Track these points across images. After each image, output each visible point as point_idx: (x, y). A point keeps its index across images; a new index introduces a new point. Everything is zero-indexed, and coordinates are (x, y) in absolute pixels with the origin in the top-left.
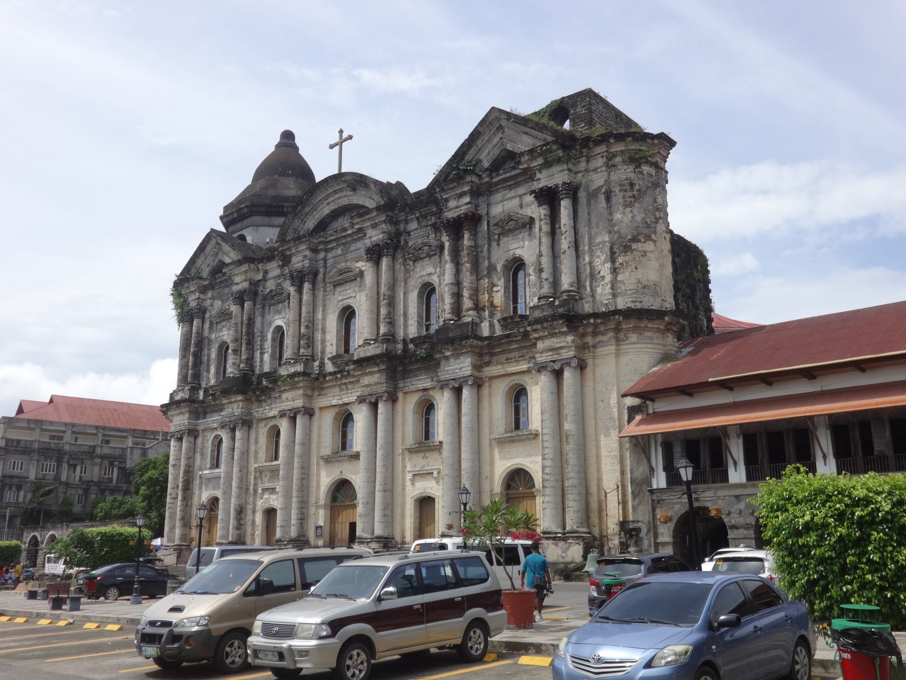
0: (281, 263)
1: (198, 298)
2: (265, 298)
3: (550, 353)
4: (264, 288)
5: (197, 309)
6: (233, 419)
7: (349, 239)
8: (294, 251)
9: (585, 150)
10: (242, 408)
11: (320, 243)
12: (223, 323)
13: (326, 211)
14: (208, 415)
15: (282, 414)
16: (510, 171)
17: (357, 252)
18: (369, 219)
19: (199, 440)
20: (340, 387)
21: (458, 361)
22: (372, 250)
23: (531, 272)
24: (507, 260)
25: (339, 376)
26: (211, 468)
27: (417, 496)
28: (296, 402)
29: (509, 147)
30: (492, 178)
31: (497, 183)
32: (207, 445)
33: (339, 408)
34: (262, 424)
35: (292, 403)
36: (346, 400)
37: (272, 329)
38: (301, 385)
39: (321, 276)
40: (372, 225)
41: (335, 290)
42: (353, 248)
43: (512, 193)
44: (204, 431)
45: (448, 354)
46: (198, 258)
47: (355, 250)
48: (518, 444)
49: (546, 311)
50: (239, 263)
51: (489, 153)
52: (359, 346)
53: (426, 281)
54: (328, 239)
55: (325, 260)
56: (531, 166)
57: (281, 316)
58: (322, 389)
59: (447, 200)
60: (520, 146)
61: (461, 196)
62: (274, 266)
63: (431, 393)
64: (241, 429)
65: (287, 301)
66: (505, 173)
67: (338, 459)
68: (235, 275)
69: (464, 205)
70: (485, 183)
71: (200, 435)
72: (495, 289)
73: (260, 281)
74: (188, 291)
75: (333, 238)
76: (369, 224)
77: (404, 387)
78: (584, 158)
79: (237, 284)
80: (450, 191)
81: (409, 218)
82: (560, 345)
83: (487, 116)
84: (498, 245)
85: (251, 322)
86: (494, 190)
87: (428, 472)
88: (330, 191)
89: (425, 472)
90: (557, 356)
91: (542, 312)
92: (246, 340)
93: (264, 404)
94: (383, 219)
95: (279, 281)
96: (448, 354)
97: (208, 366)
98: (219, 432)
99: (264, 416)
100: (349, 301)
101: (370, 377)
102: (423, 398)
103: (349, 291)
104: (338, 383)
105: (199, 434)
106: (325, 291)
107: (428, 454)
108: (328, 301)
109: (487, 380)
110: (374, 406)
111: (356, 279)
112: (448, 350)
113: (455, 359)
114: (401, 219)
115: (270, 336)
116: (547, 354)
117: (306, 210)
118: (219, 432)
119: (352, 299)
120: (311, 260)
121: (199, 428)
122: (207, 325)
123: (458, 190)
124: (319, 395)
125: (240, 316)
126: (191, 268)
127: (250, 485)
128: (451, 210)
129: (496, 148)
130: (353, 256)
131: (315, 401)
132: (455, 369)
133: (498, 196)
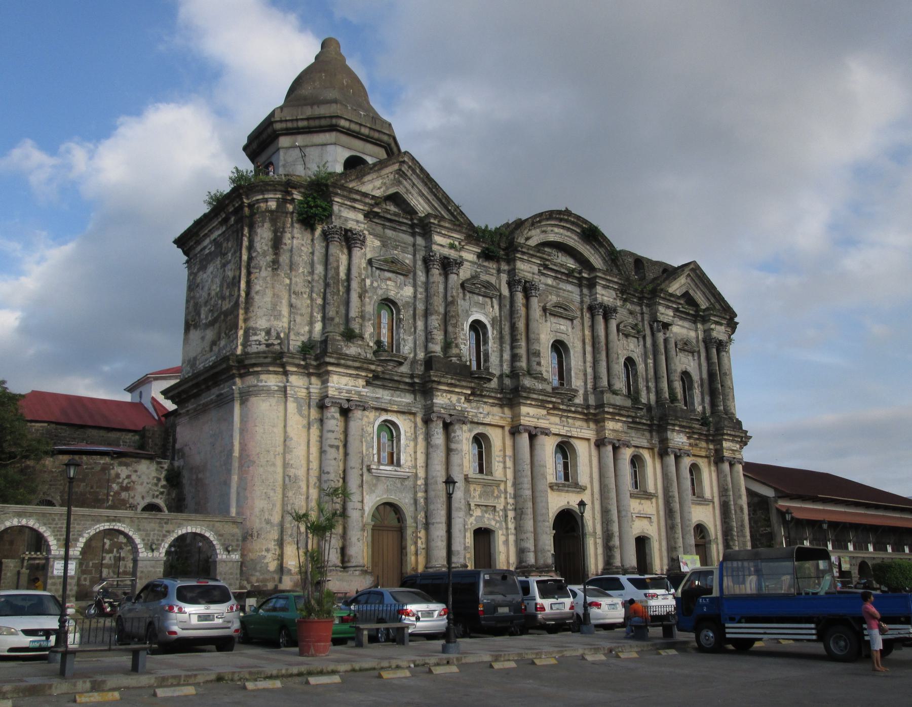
6: (452, 412)
25: (573, 409)
28: (540, 421)
32: (370, 429)
35: (536, 420)
36: (575, 434)
37: (471, 320)
38: (551, 406)
61: (668, 307)
62: (474, 249)
63: (641, 451)
74: (349, 203)
95: (479, 270)
99: (476, 420)
103: (562, 327)
107: (643, 501)
115: (466, 327)
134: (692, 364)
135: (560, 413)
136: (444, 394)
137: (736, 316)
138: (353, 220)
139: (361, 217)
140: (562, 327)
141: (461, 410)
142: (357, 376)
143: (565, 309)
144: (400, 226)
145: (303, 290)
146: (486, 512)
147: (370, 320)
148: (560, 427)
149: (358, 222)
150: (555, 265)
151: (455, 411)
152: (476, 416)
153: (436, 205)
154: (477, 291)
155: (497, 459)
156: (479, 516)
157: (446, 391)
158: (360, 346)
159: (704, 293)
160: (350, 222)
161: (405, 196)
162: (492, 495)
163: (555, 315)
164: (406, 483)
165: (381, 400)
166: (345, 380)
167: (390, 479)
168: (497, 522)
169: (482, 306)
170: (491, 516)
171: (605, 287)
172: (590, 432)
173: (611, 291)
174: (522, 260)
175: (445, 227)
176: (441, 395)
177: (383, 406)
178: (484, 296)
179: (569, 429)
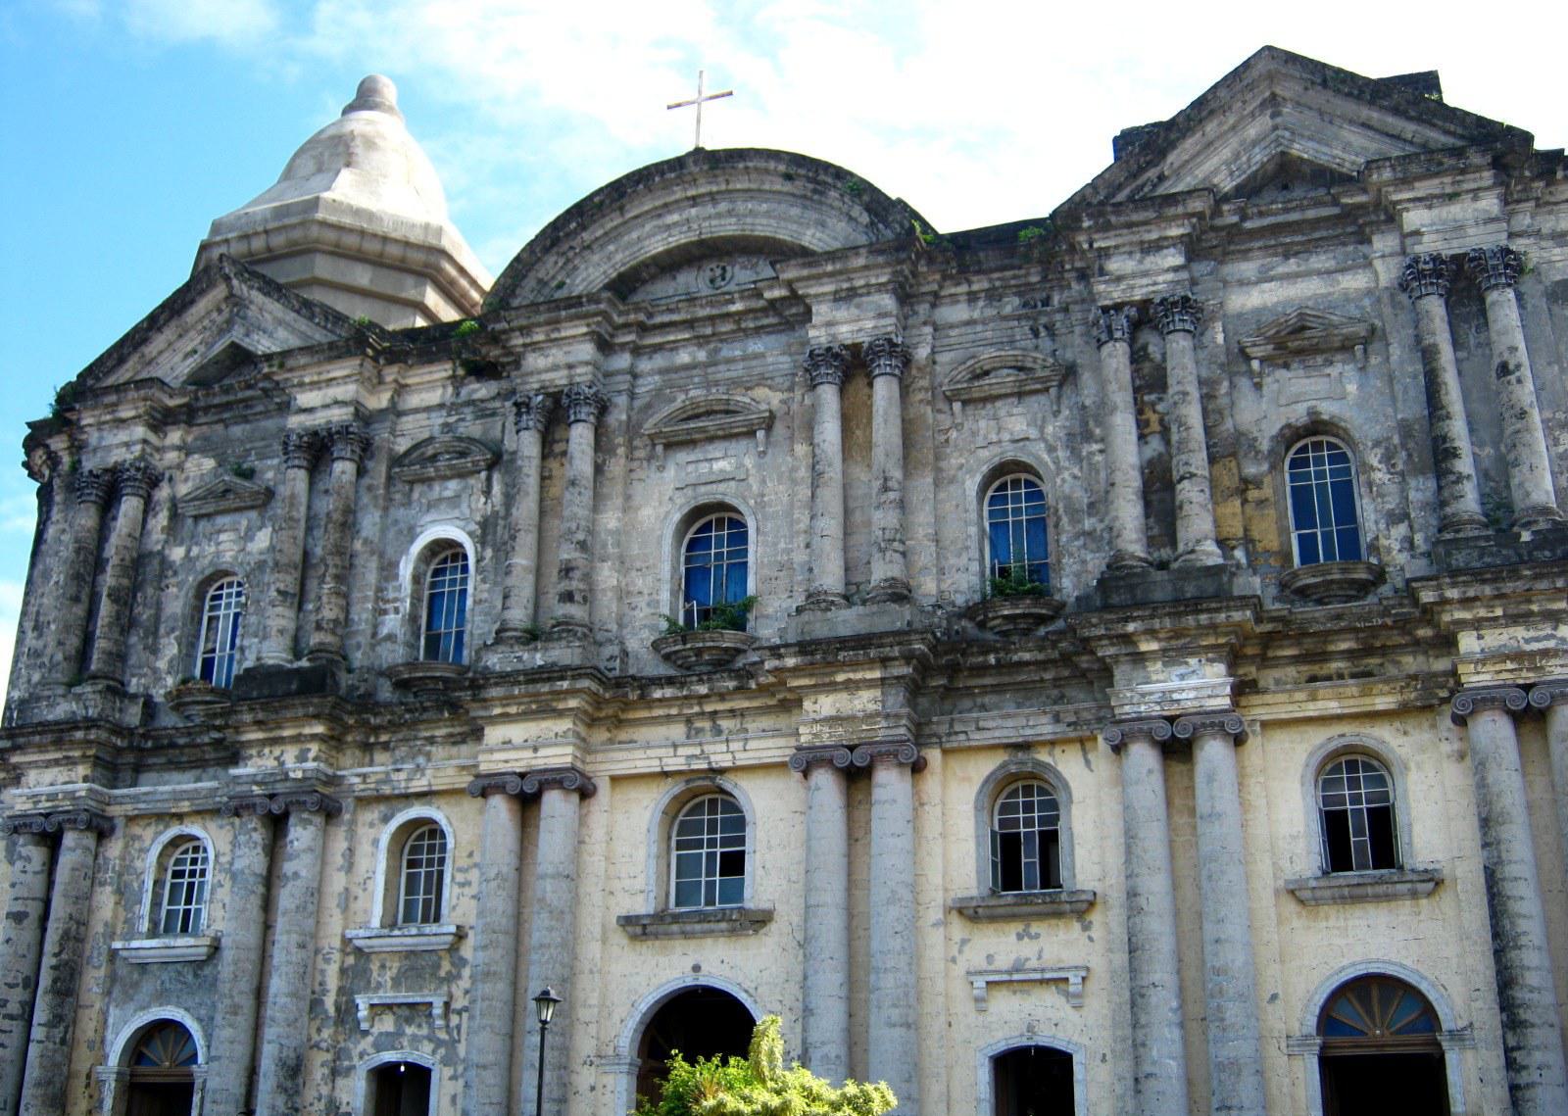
0: (461, 372)
1: (145, 441)
2: (397, 461)
3: (1510, 665)
4: (393, 432)
5: (138, 469)
6: (280, 788)
7: (726, 327)
8: (540, 337)
9: (1540, 184)
10: (315, 760)
11: (626, 325)
12: (222, 521)
13: (657, 246)
14: (144, 777)
15: (486, 787)
16: (1302, 208)
17: (754, 363)
18: (831, 275)
19: (114, 849)
20: (689, 721)
21: (1182, 670)
22: (836, 356)
23: (1374, 461)
24: (1288, 426)
25: (703, 690)
26: (153, 933)
27: (1002, 1047)
28: (542, 752)
29: (1301, 149)
30: (1244, 218)
31: (1254, 234)
32: (138, 864)
33: (688, 782)
34: (372, 814)
35: (529, 754)
36: (722, 760)
37: (417, 547)
38: (573, 703)
39: (618, 416)
40: (836, 292)
41: (665, 457)
42: (728, 351)
43: (1292, 265)
44: (131, 819)
45: (1148, 646)
46: (160, 330)
47: (744, 358)
48: (1371, 908)
49: (1491, 554)
50: (335, 352)
51: (1237, 156)
52: (799, 610)
53: (1009, 456)
54: (658, 319)
55: (635, 376)
56: (1395, 197)
57: (456, 513)
58: (619, 723)
59: (1105, 253)
60: (1337, 152)
63: (1043, 756)
64: (306, 823)
65: (483, 475)
66: (1286, 210)
67: (688, 928)
68: (301, 385)
69: (1168, 270)
70: (1223, 228)
71: (119, 832)
72: (1253, 494)
73: (382, 411)
75: (675, 317)
76: (829, 288)
77: (949, 734)
78: (1532, 204)
79: (310, 410)
80: (1125, 231)
81: (943, 293)
82: (1535, 646)
83: (1246, 65)
84: (1258, 386)
85: (348, 524)
86: (1233, 252)
87: (1048, 975)
88: (678, 195)
89: (1038, 976)
90: (1531, 675)
91: (1481, 557)
92: (336, 566)
93: (380, 757)
94: (883, 279)
96: (1148, 646)
97: (153, 632)
98: (193, 828)
99: (387, 790)
100: (722, 487)
101: (844, 695)
102: (1013, 769)
103: (718, 466)
104: (687, 711)
105: (113, 830)
106: (630, 458)
107: (1036, 927)
108: (638, 487)
109: (1258, 727)
110: (856, 777)
111: (751, 434)
112: (1152, 633)
113: (1165, 664)
114: (926, 289)
115: (406, 569)
116: (1498, 667)
117: (587, 236)
118: (193, 828)
119: (733, 484)
120: (596, 365)
121: (115, 810)
122: (161, 520)
123: (1149, 231)
124: (611, 741)
125: (303, 499)
126: (129, 354)
127: (325, 992)
128: (1119, 279)
129: (1257, 150)
130: (733, 374)
131: (600, 757)
132: (1172, 692)
133: (1248, 268)
134: (1352, 388)
135: (674, 711)
136: (266, 751)
137: (1527, 138)
138: (118, 446)
139: (140, 431)
140: (718, 466)
141: (305, 779)
142: (70, 762)
143: (727, 412)
144: (251, 407)
145: (51, 618)
146: (409, 1021)
147: (173, 630)
148: (662, 752)
149: (127, 445)
150: (671, 311)
151: (288, 784)
152: (387, 781)
153: (303, 328)
154: (431, 471)
155: (460, 877)
156: (388, 1034)
157: (264, 743)
158: (78, 697)
159: (1366, 126)
160: (116, 451)
161: (246, 343)
162: (434, 975)
163: (690, 443)
164: (207, 971)
165: (158, 797)
166: (50, 775)
167: (170, 967)
168: (439, 1043)
169: (454, 501)
170: (425, 1031)
171: (841, 298)
172: (781, 742)
173: (876, 298)
174: (534, 347)
175: (304, 367)
176: (260, 755)
177: (160, 807)
178: (462, 475)
179: (697, 751)
